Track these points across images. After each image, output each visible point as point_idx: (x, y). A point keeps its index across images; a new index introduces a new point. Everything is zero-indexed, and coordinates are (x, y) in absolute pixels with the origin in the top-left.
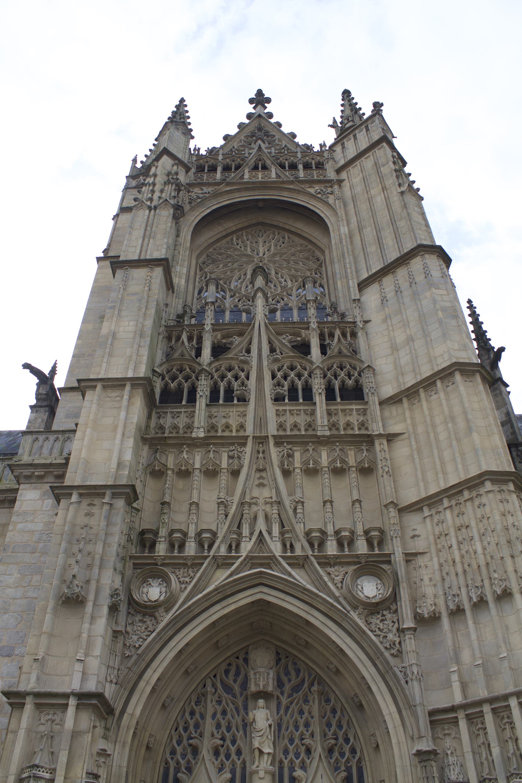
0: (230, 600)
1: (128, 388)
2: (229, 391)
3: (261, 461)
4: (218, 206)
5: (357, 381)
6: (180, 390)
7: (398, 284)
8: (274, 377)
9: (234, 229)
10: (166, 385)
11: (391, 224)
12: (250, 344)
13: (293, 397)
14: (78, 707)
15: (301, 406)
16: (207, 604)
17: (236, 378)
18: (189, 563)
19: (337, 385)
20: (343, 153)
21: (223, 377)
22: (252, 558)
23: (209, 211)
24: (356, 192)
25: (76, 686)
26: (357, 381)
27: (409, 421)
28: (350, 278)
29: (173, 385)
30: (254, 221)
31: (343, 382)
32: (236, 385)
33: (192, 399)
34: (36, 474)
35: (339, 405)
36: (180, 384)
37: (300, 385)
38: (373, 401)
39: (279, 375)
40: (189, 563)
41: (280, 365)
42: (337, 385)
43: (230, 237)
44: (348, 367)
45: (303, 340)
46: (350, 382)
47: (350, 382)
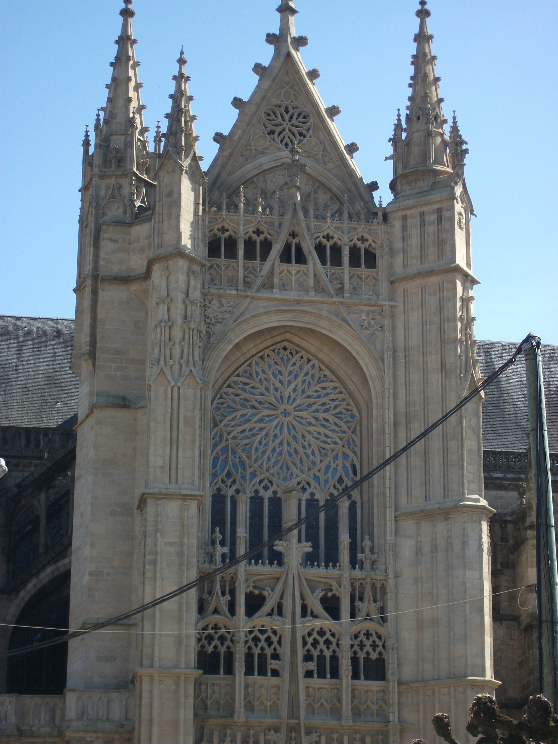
2: (262, 656)
5: (380, 654)
6: (216, 654)
7: (436, 539)
8: (305, 643)
11: (442, 451)
12: (281, 597)
13: (322, 675)
15: (327, 682)
17: (270, 643)
20: (403, 242)
21: (256, 640)
24: (410, 344)
26: (380, 654)
27: (421, 715)
28: (388, 505)
29: (210, 649)
31: (368, 653)
32: (269, 652)
33: (229, 670)
34: (88, 739)
35: (363, 684)
36: (215, 647)
37: (328, 654)
38: (393, 685)
39: (310, 640)
42: (362, 656)
44: (375, 636)
45: (334, 596)
46: (374, 656)
47: (374, 656)
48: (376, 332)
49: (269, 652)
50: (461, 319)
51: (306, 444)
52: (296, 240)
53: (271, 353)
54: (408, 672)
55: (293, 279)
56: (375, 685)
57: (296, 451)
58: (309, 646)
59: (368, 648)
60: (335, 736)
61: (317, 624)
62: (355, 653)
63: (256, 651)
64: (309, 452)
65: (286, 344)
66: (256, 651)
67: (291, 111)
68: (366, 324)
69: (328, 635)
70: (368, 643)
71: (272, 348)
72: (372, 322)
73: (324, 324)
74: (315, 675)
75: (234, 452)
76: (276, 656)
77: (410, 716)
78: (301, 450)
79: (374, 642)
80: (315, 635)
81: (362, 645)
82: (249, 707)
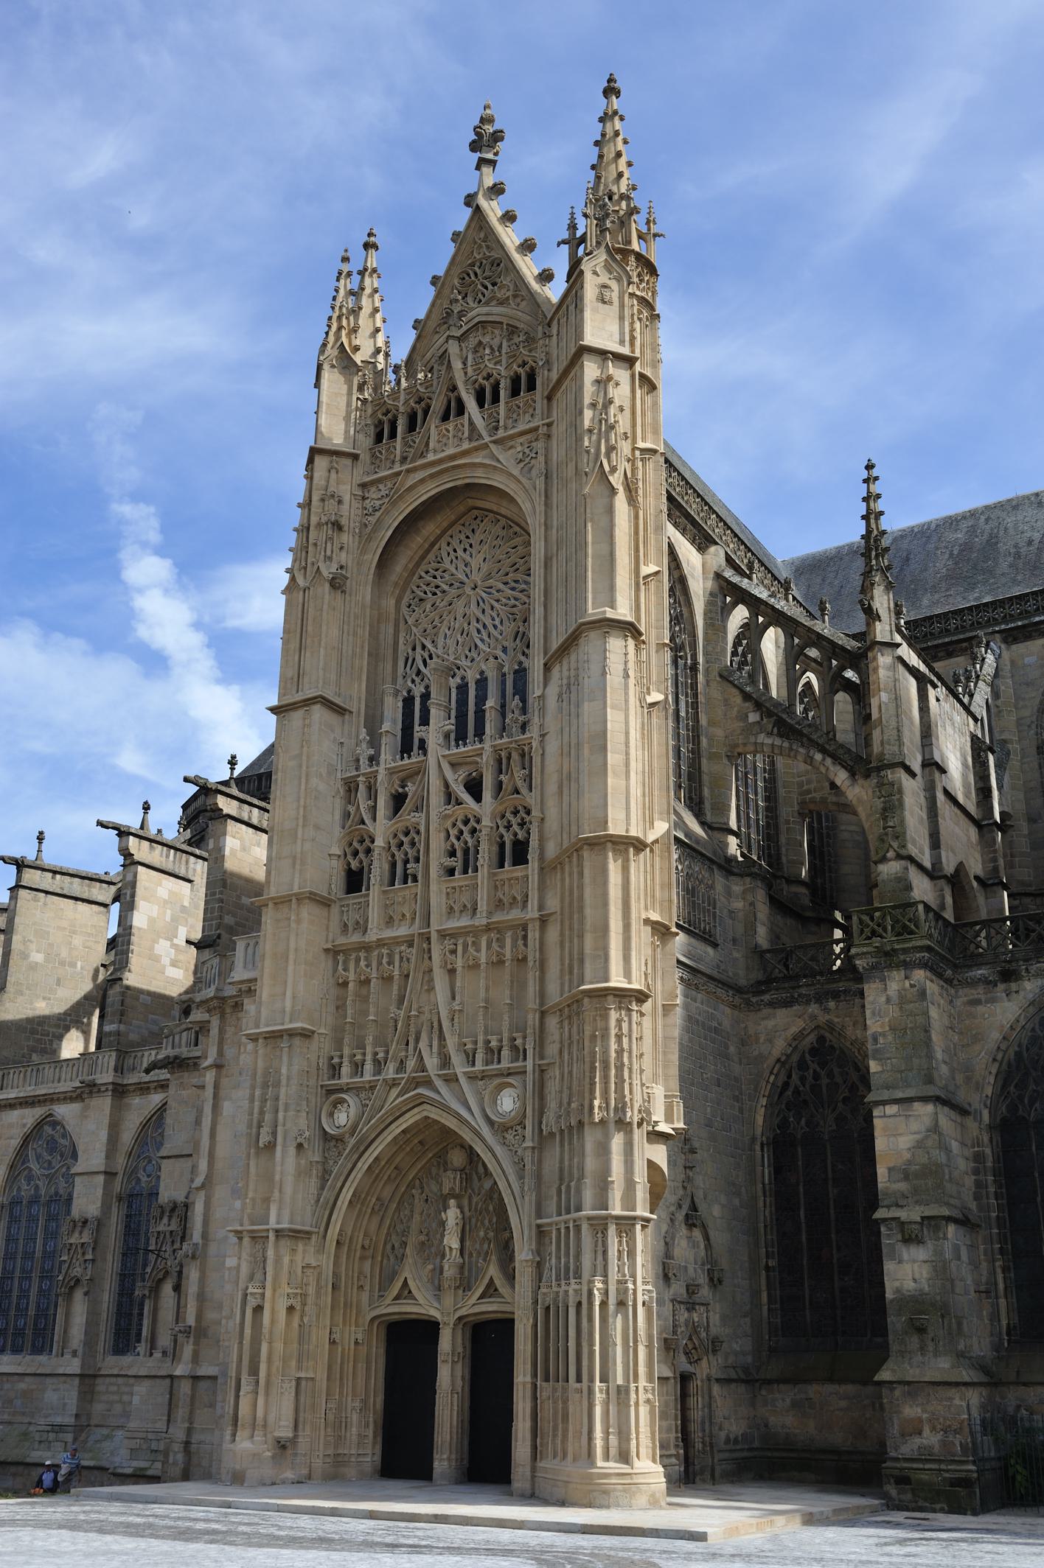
0: (401, 1120)
1: (294, 906)
3: (426, 961)
4: (401, 518)
9: (438, 532)
10: (349, 864)
14: (277, 1236)
16: (382, 1126)
18: (367, 1086)
19: (508, 839)
22: (414, 1078)
23: (390, 533)
25: (273, 1223)
30: (462, 508)
31: (516, 834)
32: (411, 853)
39: (453, 832)
40: (367, 1086)
41: (453, 819)
42: (508, 839)
43: (437, 547)
48: (533, 461)
49: (411, 853)
50: (593, 405)
51: (494, 614)
52: (455, 393)
53: (461, 528)
54: (552, 850)
55: (450, 435)
56: (519, 871)
57: (485, 627)
58: (453, 839)
59: (515, 827)
60: (470, 940)
61: (459, 813)
62: (502, 836)
63: (399, 857)
64: (497, 622)
65: (476, 512)
66: (399, 857)
67: (484, 262)
68: (520, 456)
69: (472, 823)
70: (514, 821)
71: (461, 521)
72: (527, 451)
73: (480, 473)
74: (456, 873)
75: (424, 647)
76: (417, 860)
77: (553, 904)
78: (488, 622)
79: (523, 819)
80: (460, 824)
81: (508, 827)
82: (390, 922)
